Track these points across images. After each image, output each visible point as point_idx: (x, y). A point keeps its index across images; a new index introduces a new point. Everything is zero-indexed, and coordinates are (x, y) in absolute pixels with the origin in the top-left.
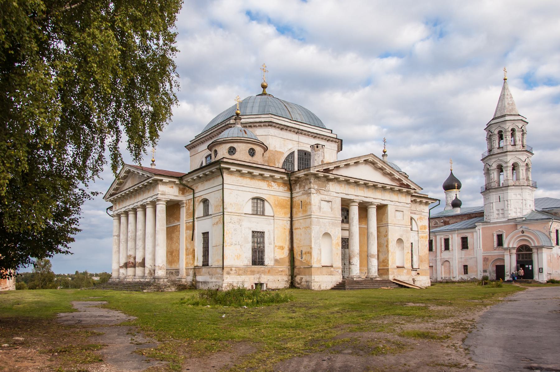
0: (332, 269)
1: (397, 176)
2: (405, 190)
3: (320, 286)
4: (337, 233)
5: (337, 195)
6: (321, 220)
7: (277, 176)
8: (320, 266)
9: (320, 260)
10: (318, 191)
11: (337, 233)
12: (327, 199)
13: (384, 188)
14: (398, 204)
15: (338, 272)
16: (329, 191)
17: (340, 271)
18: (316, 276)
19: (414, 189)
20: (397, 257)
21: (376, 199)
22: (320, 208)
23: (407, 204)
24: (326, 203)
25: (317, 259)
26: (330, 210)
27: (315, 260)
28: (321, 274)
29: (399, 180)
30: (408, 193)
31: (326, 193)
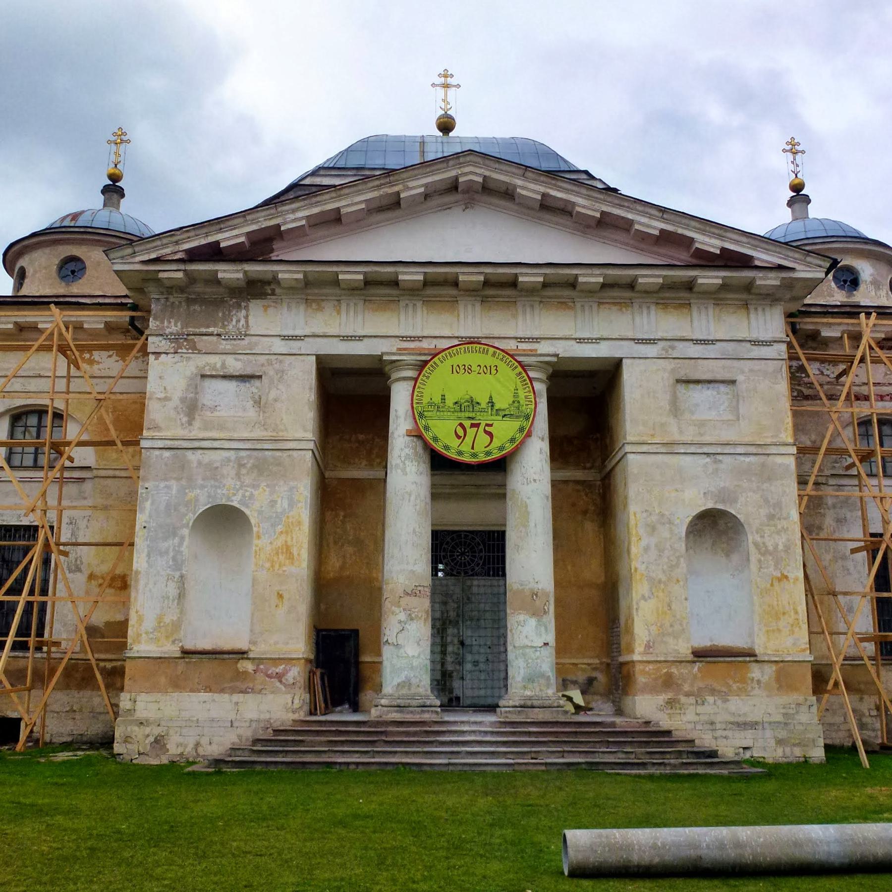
0: (249, 666)
1: (655, 226)
2: (710, 278)
3: (159, 742)
4: (282, 504)
5: (295, 346)
6: (191, 456)
7: (93, 320)
8: (172, 649)
9: (177, 626)
10: (183, 342)
11: (282, 504)
12: (234, 365)
13: (559, 287)
14: (694, 351)
15: (279, 677)
16: (242, 335)
17: (296, 673)
18: (142, 698)
19: (780, 268)
20: (673, 603)
21: (536, 340)
22: (192, 408)
23: (756, 343)
24: (232, 385)
25: (160, 619)
26: (252, 413)
27: (149, 624)
28: (177, 684)
29: (666, 239)
30: (747, 297)
31: (225, 345)
